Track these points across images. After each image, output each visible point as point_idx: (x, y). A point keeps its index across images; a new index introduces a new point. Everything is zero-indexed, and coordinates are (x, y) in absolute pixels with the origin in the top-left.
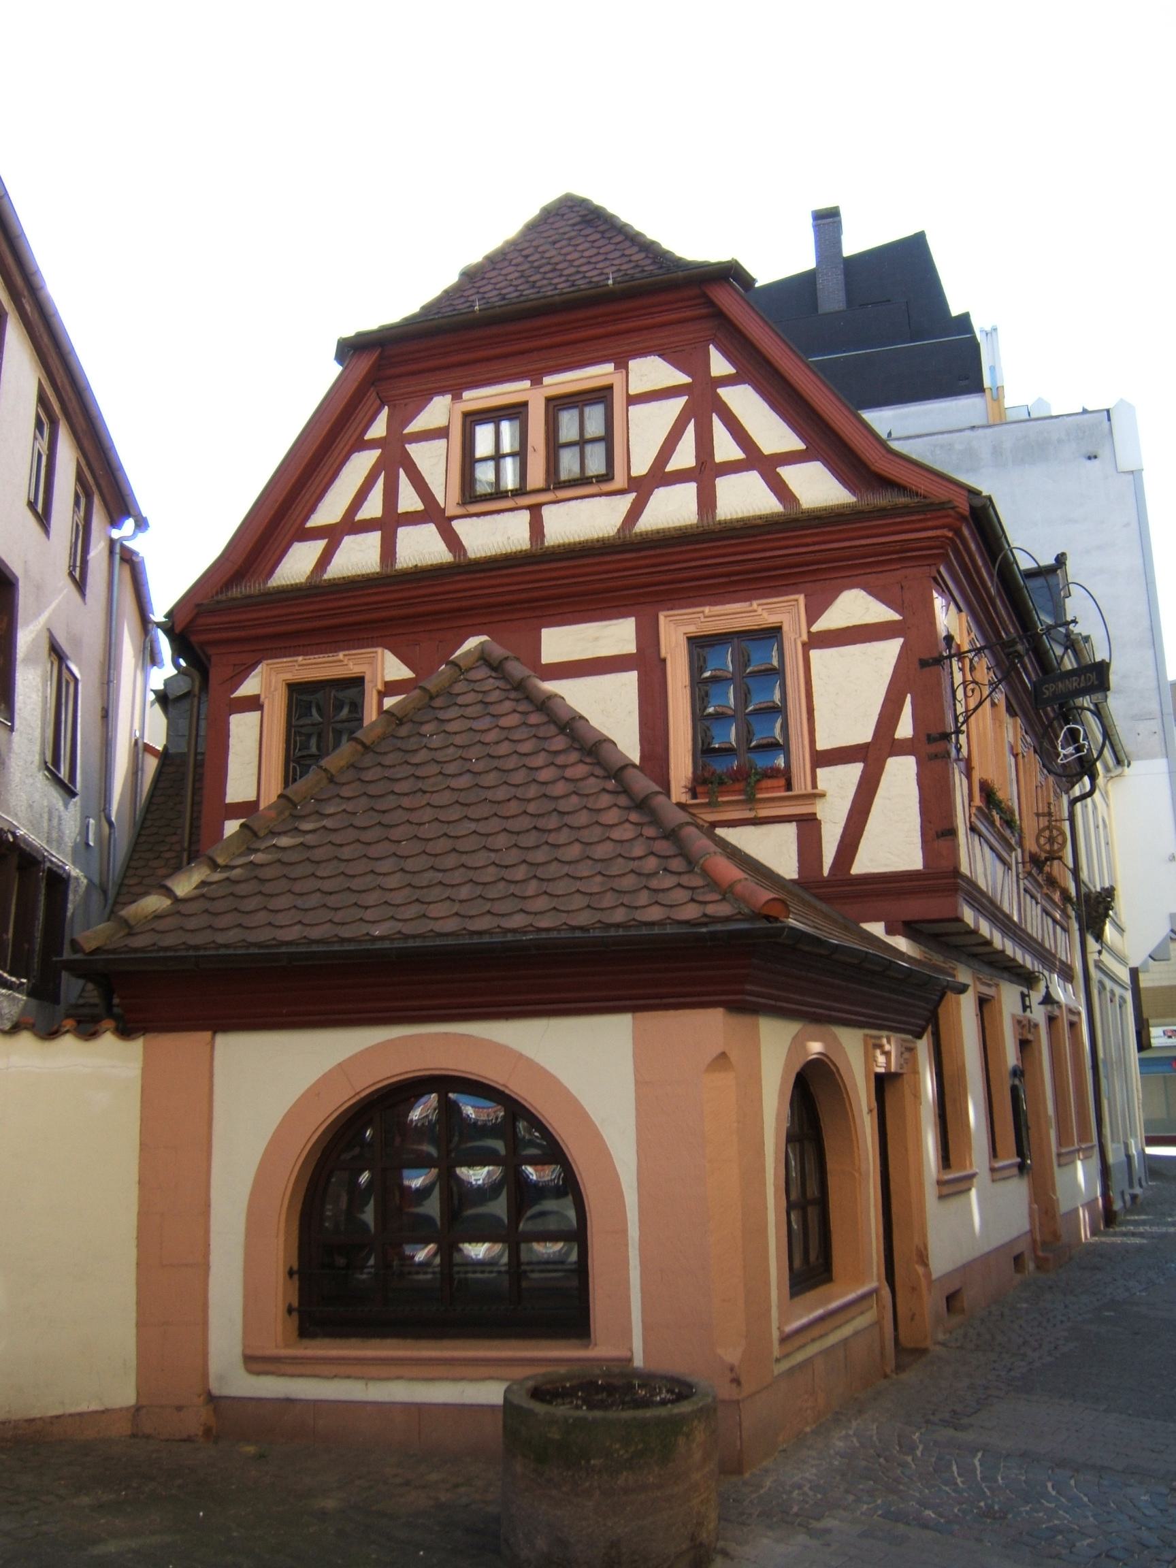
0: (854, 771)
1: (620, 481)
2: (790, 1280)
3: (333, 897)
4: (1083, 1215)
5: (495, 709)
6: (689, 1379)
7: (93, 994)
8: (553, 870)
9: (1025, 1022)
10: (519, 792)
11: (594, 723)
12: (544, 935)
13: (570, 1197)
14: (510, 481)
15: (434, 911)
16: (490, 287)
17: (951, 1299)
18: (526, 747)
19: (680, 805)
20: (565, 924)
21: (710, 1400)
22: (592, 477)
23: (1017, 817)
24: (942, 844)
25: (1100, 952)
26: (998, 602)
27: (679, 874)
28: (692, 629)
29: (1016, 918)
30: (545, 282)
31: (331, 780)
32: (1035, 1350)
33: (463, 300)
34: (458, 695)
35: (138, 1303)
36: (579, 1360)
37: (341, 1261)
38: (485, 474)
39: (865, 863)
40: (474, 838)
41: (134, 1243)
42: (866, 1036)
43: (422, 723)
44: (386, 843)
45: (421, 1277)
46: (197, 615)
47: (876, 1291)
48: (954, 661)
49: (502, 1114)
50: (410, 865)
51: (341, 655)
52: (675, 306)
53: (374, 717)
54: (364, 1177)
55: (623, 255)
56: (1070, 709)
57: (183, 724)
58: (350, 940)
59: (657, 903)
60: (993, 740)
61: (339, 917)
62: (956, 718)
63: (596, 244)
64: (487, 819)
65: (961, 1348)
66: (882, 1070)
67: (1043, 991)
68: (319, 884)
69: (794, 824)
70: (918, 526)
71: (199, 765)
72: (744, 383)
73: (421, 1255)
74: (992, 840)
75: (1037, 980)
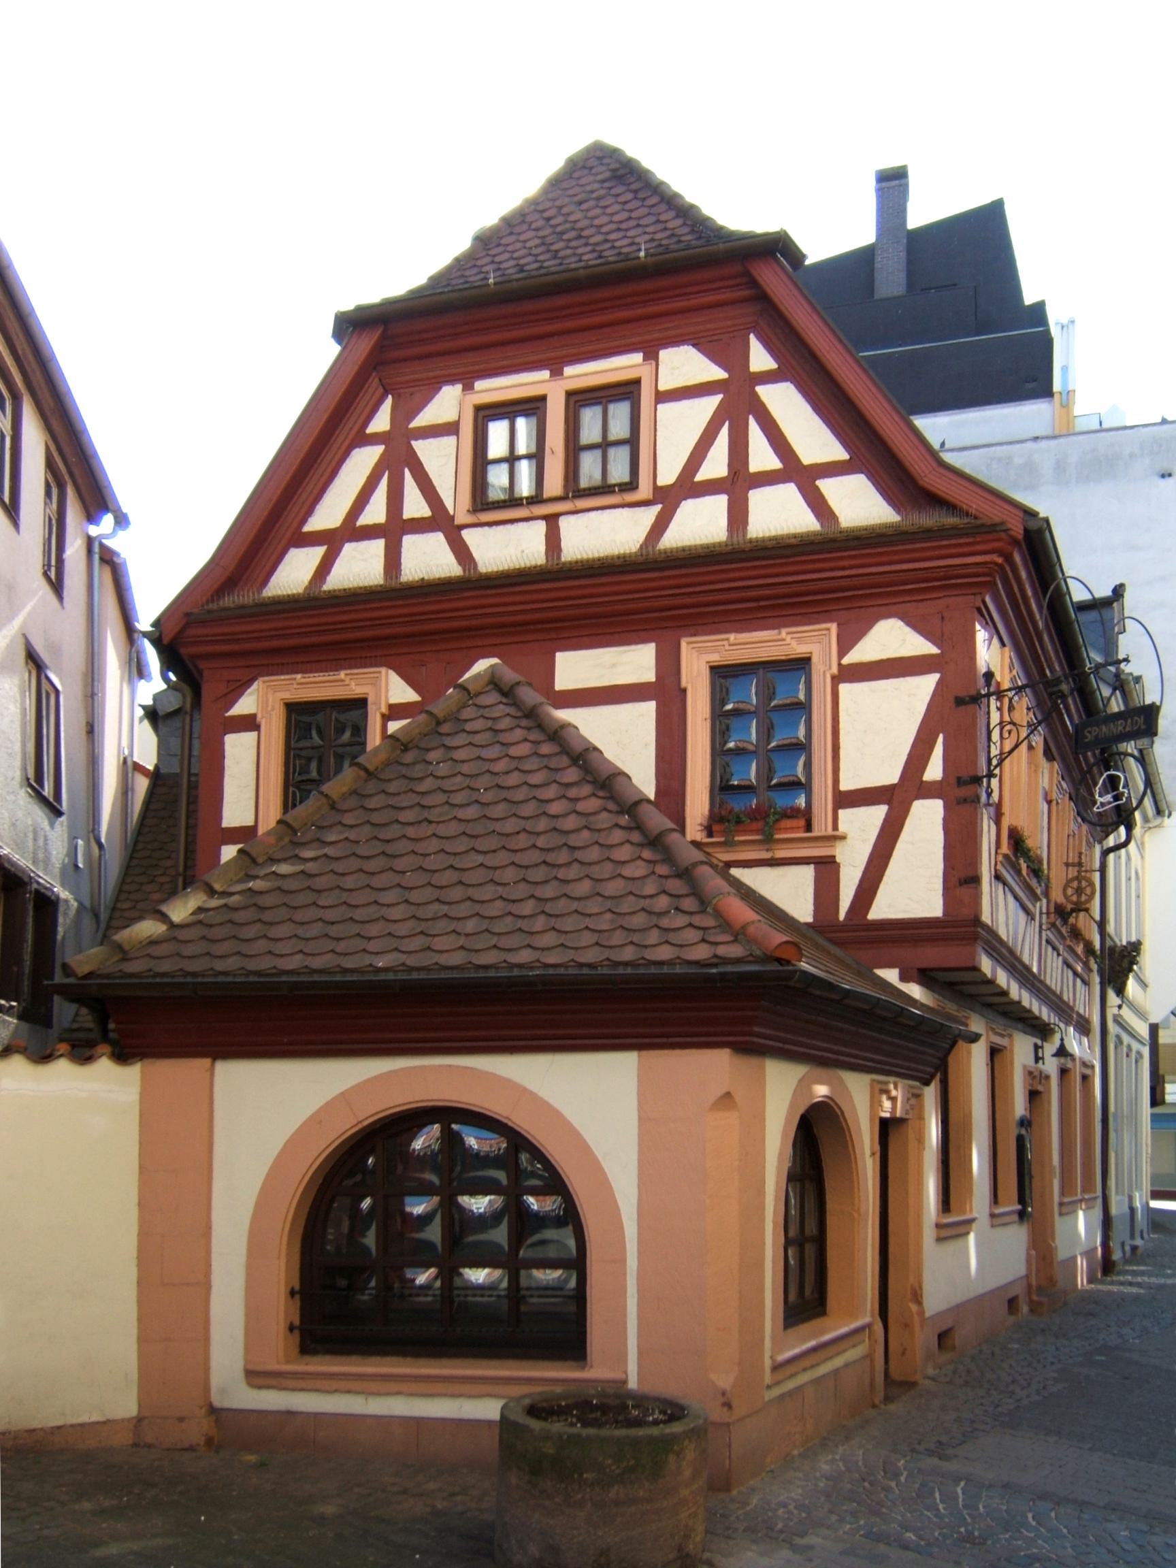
0: (879, 813)
1: (644, 491)
2: (785, 1312)
3: (335, 927)
4: (1082, 1263)
5: (503, 737)
6: (682, 1402)
7: (87, 1018)
8: (562, 905)
9: (1037, 1073)
10: (529, 825)
11: (608, 754)
12: (551, 971)
13: (570, 1227)
14: (525, 487)
15: (439, 943)
16: (506, 256)
17: (943, 1337)
18: (536, 779)
19: (695, 843)
20: (572, 960)
21: (701, 1421)
22: (614, 485)
23: (1045, 866)
24: (964, 892)
25: (1120, 1007)
26: (1046, 637)
27: (691, 913)
28: (715, 658)
29: (1035, 970)
30: (569, 252)
31: (333, 806)
32: (1023, 1389)
33: (475, 271)
34: (466, 721)
35: (140, 1320)
36: (575, 1380)
37: (343, 1283)
38: (498, 477)
39: (883, 909)
40: (481, 870)
41: (134, 1262)
42: (873, 1081)
43: (428, 750)
44: (391, 874)
45: (421, 1299)
46: (187, 625)
47: (869, 1326)
48: (993, 700)
49: (505, 1145)
50: (415, 896)
51: (342, 674)
52: (714, 286)
53: (378, 742)
54: (366, 1203)
55: (658, 221)
56: (1112, 755)
57: (175, 743)
58: (352, 971)
59: (667, 942)
60: (1027, 785)
61: (341, 947)
62: (989, 760)
63: (628, 207)
64: (494, 851)
65: (950, 1382)
66: (887, 1115)
67: (1057, 1043)
68: (320, 913)
69: (812, 866)
70: (966, 550)
71: (193, 787)
72: (785, 380)
73: (422, 1278)
74: (1017, 889)
75: (1052, 1032)
